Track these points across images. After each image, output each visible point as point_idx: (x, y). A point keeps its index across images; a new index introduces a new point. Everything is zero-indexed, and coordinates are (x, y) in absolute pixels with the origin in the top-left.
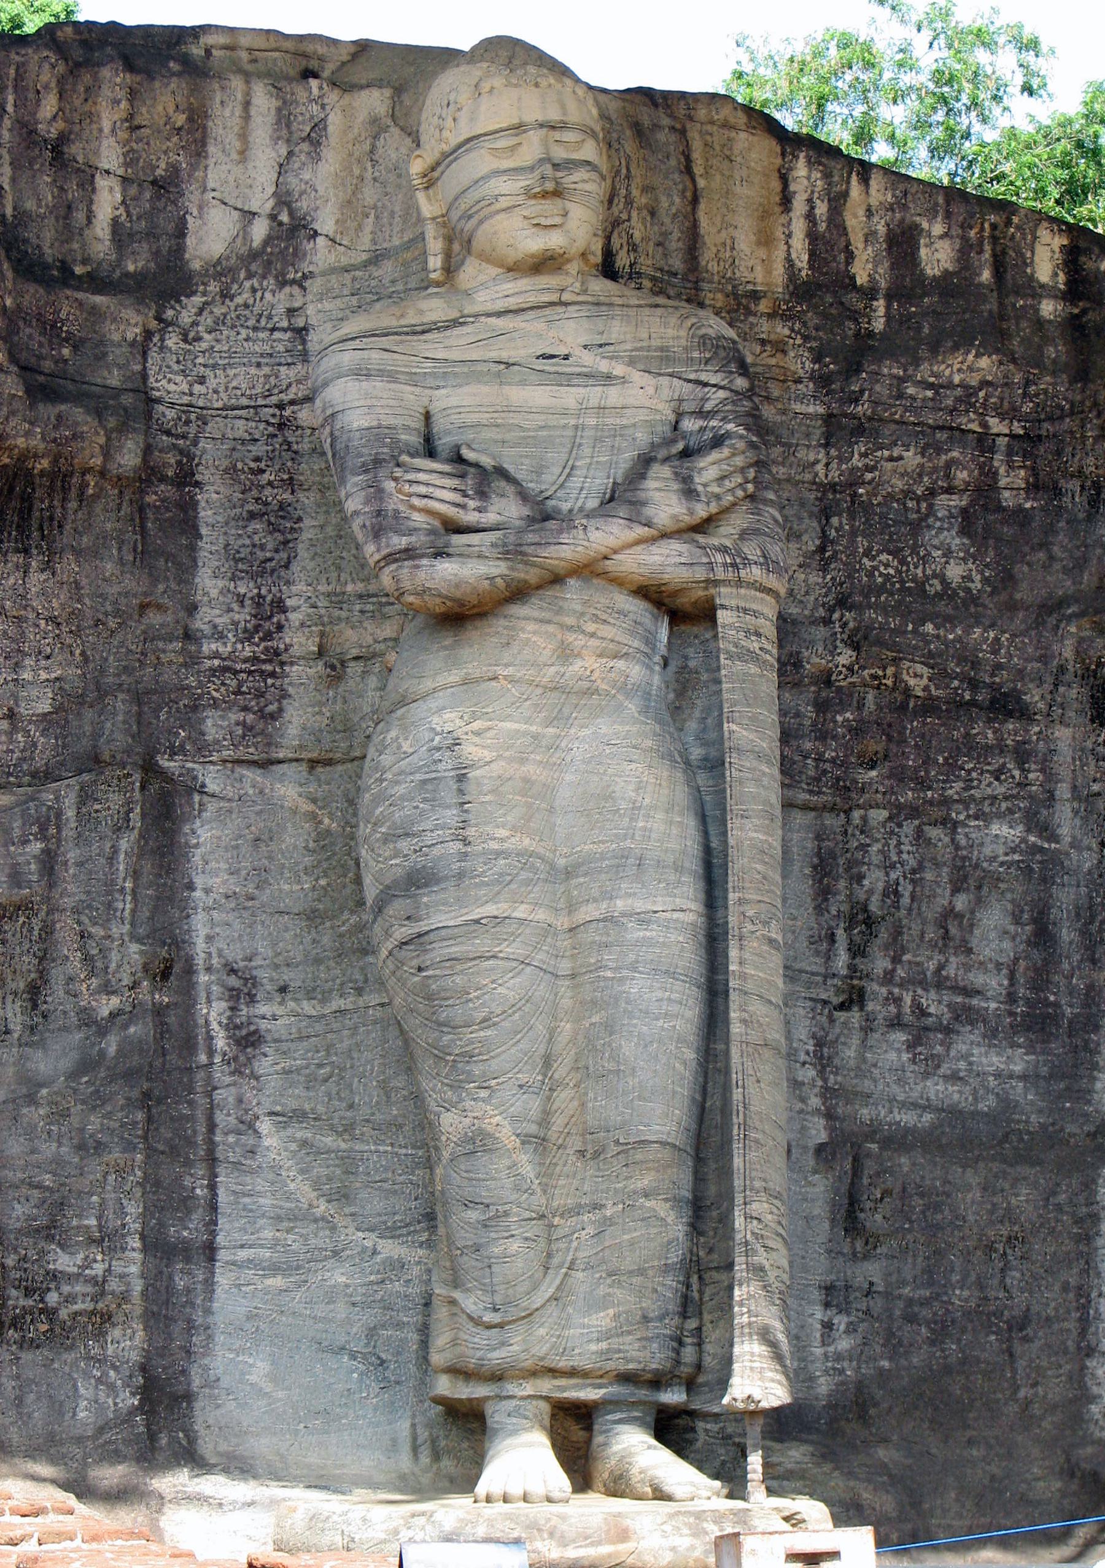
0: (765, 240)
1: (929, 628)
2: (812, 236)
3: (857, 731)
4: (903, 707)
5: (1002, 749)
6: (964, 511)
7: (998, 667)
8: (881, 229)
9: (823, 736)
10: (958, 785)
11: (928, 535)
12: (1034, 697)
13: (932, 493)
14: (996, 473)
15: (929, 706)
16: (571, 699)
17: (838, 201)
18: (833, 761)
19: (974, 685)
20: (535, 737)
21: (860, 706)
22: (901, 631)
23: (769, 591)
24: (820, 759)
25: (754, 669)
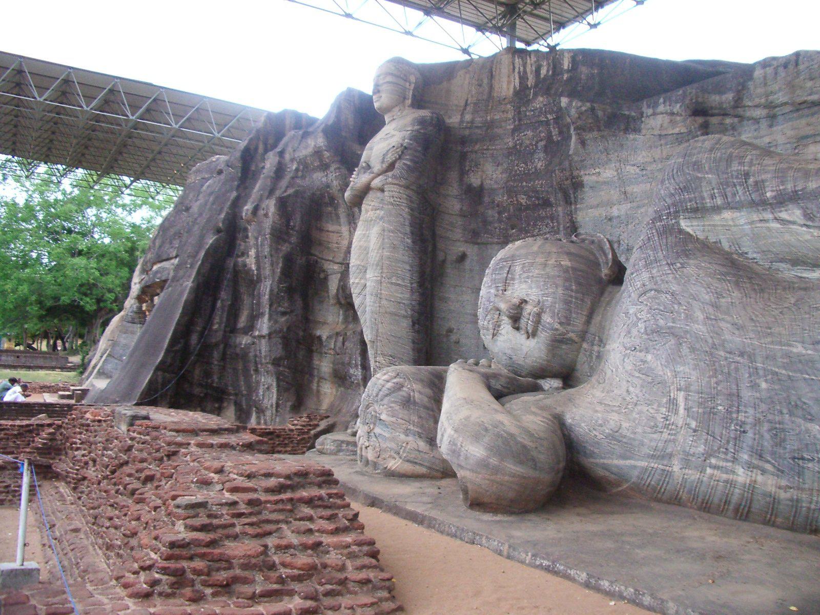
0: (509, 82)
1: (524, 184)
2: (520, 78)
3: (509, 218)
4: (520, 209)
5: (547, 217)
6: (545, 146)
7: (542, 191)
8: (534, 69)
9: (500, 221)
10: (537, 231)
11: (536, 156)
12: (552, 199)
13: (537, 142)
14: (551, 132)
15: (527, 207)
16: (369, 222)
17: (525, 65)
18: (503, 229)
19: (538, 199)
20: (364, 235)
21: (509, 210)
22: (517, 186)
23: (395, 184)
24: (500, 229)
25: (390, 207)
